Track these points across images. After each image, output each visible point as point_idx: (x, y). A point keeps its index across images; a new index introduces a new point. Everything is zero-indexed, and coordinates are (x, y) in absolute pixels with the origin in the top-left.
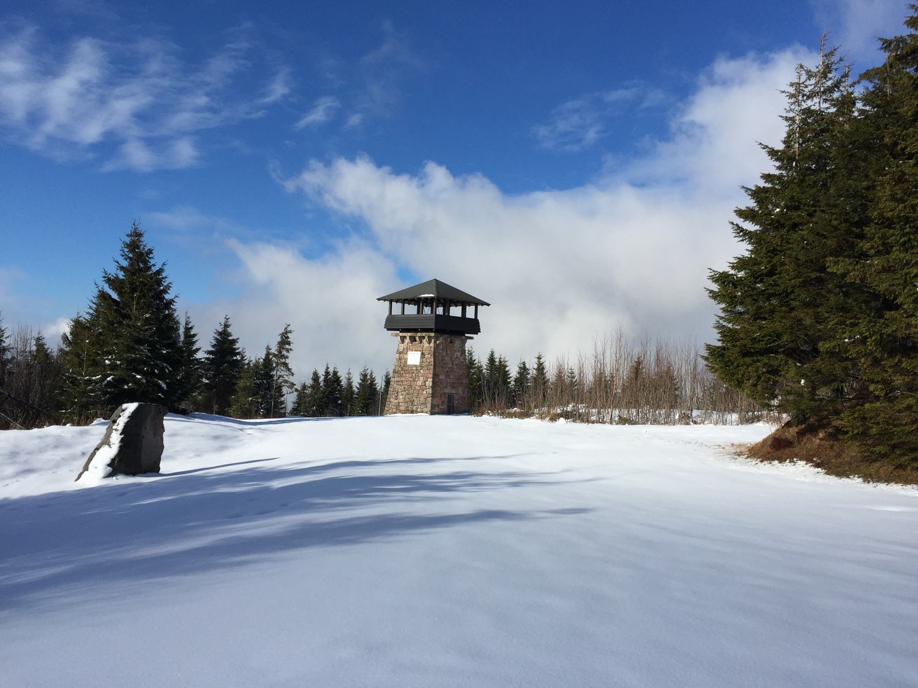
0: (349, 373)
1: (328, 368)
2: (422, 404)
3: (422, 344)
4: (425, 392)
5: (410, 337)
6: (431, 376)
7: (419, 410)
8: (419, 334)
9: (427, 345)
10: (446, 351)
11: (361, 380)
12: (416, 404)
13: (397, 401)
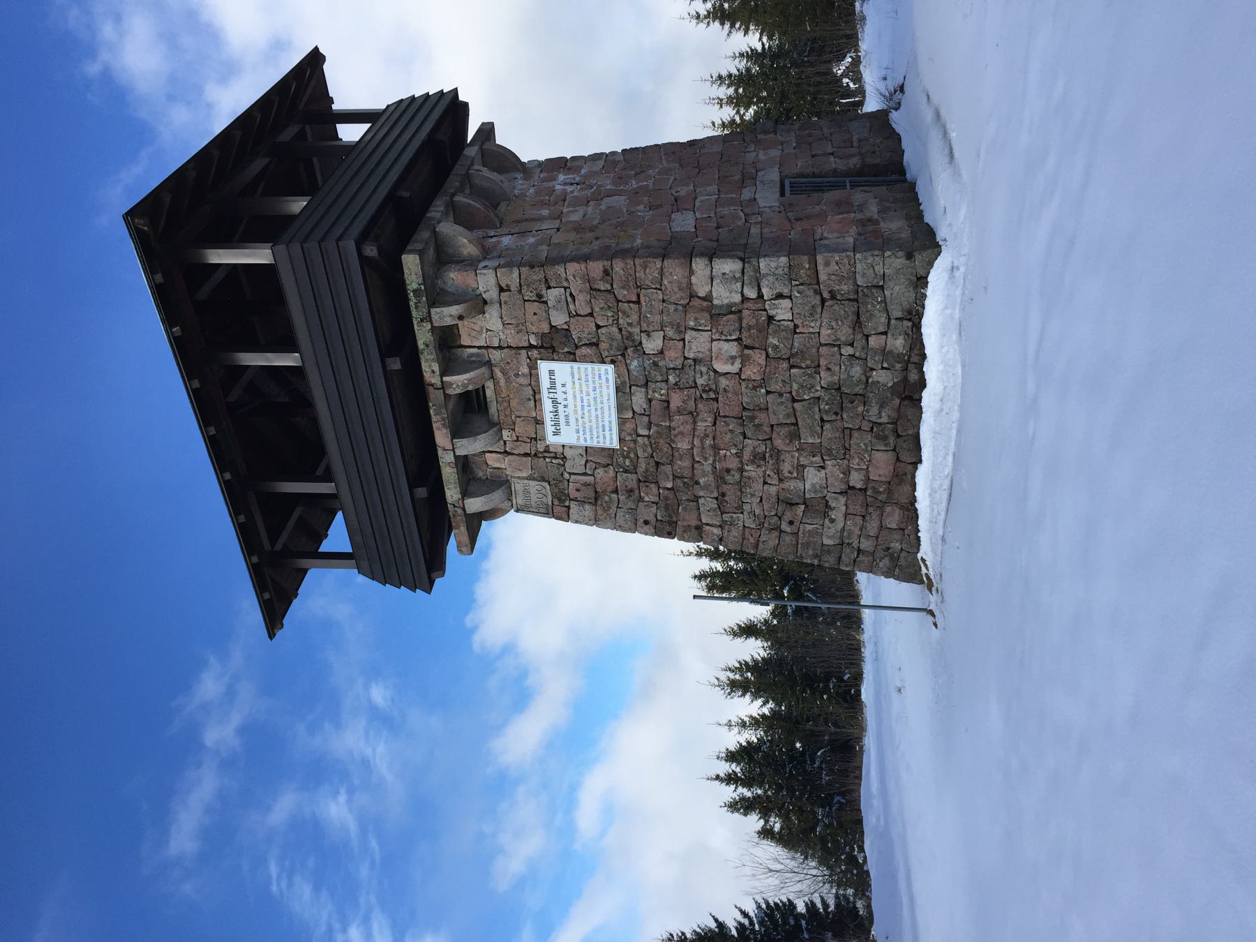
0: (729, 725)
1: (718, 777)
2: (858, 324)
3: (496, 356)
4: (782, 312)
5: (457, 432)
6: (674, 271)
7: (898, 344)
8: (430, 368)
10: (541, 219)
11: (743, 695)
12: (857, 371)
13: (839, 506)
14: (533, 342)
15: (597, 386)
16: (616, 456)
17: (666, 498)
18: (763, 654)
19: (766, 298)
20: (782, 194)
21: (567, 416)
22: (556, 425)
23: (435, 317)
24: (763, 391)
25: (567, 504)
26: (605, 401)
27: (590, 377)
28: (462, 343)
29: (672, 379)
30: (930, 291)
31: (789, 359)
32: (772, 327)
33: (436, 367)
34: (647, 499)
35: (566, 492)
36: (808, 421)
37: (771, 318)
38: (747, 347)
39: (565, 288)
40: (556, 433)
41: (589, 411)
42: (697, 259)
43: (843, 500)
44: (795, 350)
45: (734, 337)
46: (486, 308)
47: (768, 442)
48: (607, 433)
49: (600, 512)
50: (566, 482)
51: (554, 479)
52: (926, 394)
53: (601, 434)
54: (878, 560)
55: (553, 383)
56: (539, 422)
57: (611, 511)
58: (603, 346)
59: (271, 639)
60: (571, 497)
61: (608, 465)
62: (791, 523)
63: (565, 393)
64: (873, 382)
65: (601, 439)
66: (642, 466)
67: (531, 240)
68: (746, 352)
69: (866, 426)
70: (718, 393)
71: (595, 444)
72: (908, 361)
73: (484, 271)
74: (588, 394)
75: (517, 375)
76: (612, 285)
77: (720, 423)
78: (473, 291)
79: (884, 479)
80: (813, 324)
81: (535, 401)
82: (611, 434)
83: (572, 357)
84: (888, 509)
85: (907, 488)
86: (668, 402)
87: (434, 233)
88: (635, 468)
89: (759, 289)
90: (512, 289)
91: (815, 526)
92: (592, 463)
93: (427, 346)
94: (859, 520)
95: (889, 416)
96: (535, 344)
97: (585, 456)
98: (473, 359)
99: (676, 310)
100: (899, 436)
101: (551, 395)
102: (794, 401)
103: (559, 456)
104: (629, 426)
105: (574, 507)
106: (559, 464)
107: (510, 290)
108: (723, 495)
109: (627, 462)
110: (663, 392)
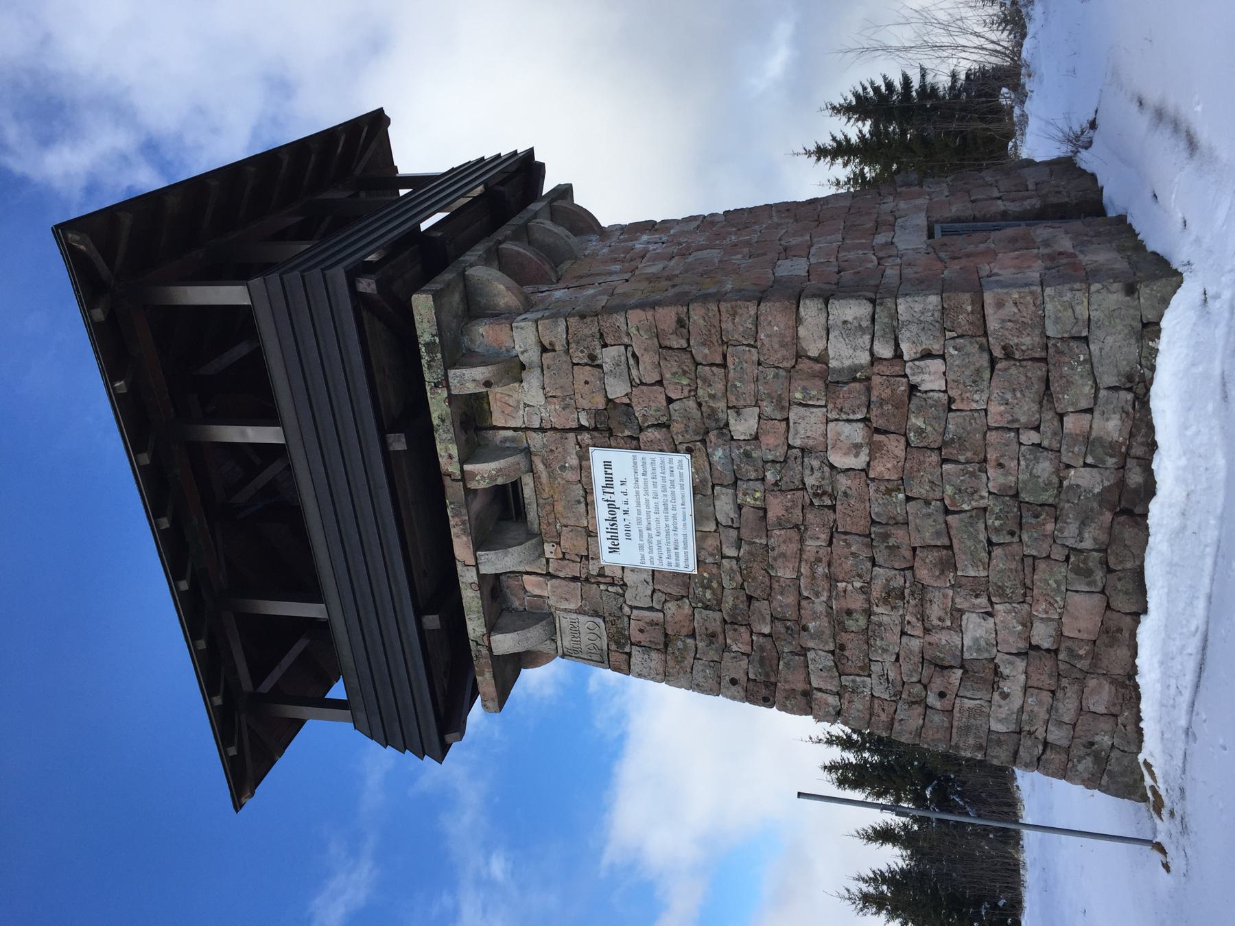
2: (1047, 393)
3: (536, 440)
4: (931, 378)
5: (481, 543)
6: (775, 320)
7: (1111, 427)
8: (447, 450)
9: (531, 391)
10: (611, 273)
11: (878, 912)
12: (1044, 468)
13: (1015, 673)
14: (584, 422)
15: (668, 484)
16: (692, 585)
17: (762, 649)
18: (902, 864)
19: (906, 357)
20: (931, 235)
21: (627, 526)
22: (614, 538)
23: (453, 382)
24: (901, 496)
25: (627, 649)
26: (679, 507)
27: (658, 470)
28: (494, 424)
29: (770, 476)
30: (1163, 344)
31: (940, 449)
32: (915, 401)
33: (454, 450)
34: (734, 648)
35: (626, 633)
36: (969, 543)
37: (913, 388)
38: (878, 431)
39: (626, 346)
40: (614, 550)
41: (657, 520)
42: (807, 302)
43: (1021, 664)
44: (949, 436)
45: (859, 416)
46: (524, 374)
47: (909, 573)
48: (681, 552)
49: (671, 663)
50: (626, 619)
51: (610, 614)
52: (1155, 507)
53: (673, 552)
54: (1075, 760)
56: (591, 534)
57: (686, 662)
58: (676, 427)
59: (237, 811)
60: (633, 640)
61: (683, 597)
62: (942, 695)
63: (625, 494)
64: (1070, 487)
65: (673, 561)
66: (728, 602)
67: (591, 291)
68: (877, 437)
69: (1058, 554)
70: (836, 499)
71: (664, 567)
72: (1127, 455)
73: (522, 324)
74: (656, 497)
75: (563, 468)
76: (688, 341)
77: (838, 543)
78: (508, 351)
79: (1085, 636)
80: (976, 397)
81: (587, 505)
82: (686, 553)
83: (634, 443)
84: (1092, 683)
85: (1124, 652)
86: (765, 510)
87: (463, 276)
88: (719, 603)
89: (897, 345)
90: (557, 348)
91: (978, 702)
92: (660, 594)
93: (443, 421)
94: (1046, 697)
95: (1095, 539)
96: (587, 425)
98: (508, 444)
99: (776, 376)
100: (1110, 571)
101: (607, 496)
102: (947, 512)
103: (617, 582)
104: (711, 542)
105: (637, 656)
106: (617, 594)
107: (554, 350)
108: (842, 647)
109: (708, 595)
110: (758, 495)
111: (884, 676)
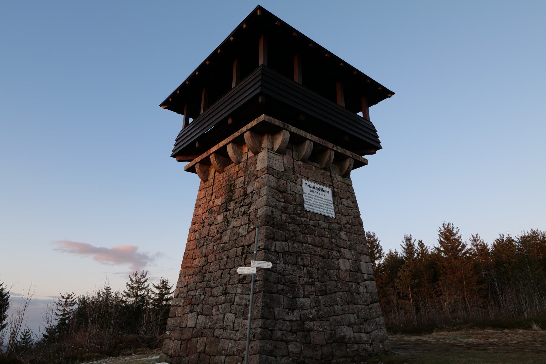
13: (295, 315)
54: (269, 343)
55: (324, 191)
62: (283, 290)
70: (332, 259)
79: (312, 340)
82: (310, 208)
91: (283, 303)
94: (289, 329)
97: (299, 193)
108: (291, 255)
110: (328, 236)
111: (285, 269)
